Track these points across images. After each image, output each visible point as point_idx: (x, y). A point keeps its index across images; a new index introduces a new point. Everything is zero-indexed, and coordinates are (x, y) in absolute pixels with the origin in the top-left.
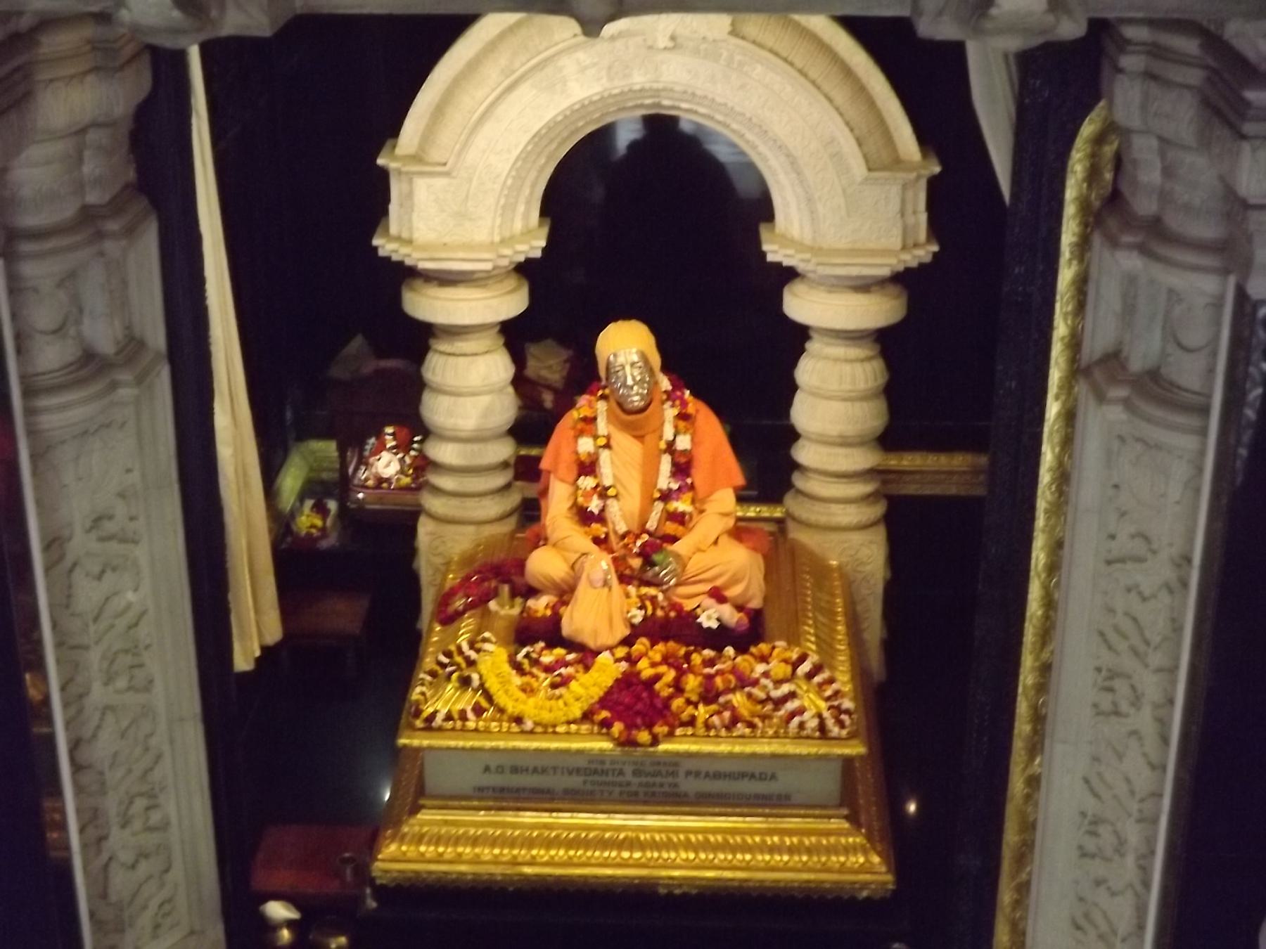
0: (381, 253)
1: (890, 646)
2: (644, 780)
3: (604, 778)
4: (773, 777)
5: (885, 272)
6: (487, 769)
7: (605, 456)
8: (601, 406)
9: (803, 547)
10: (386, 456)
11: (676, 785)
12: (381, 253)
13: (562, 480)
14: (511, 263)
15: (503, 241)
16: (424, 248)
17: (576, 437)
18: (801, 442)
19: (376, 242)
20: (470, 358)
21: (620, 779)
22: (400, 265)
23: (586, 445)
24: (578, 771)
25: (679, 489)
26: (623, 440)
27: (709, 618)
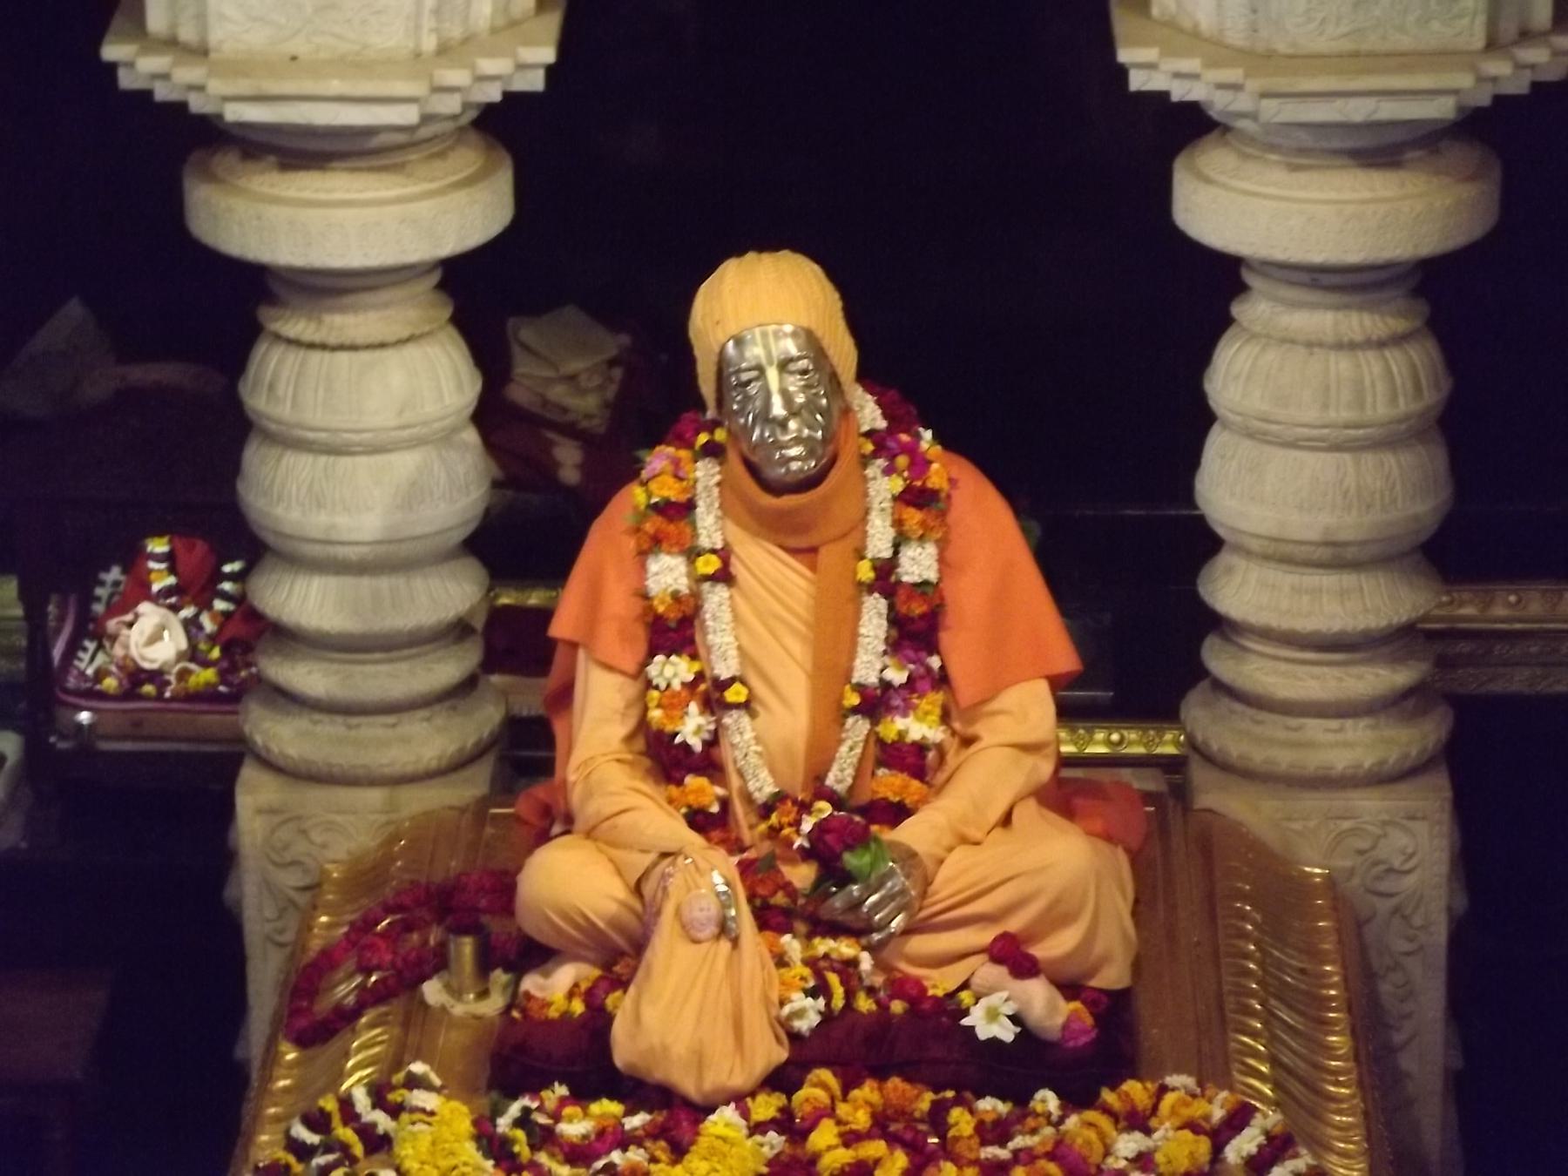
0: (126, 81)
1: (1464, 1087)
5: (1442, 109)
7: (716, 599)
8: (706, 473)
9: (1235, 830)
10: (149, 615)
12: (126, 81)
13: (610, 668)
14: (466, 106)
15: (443, 50)
16: (240, 67)
17: (643, 554)
18: (1224, 559)
19: (111, 51)
20: (364, 356)
22: (178, 109)
23: (667, 574)
25: (910, 684)
26: (760, 560)
27: (992, 1015)
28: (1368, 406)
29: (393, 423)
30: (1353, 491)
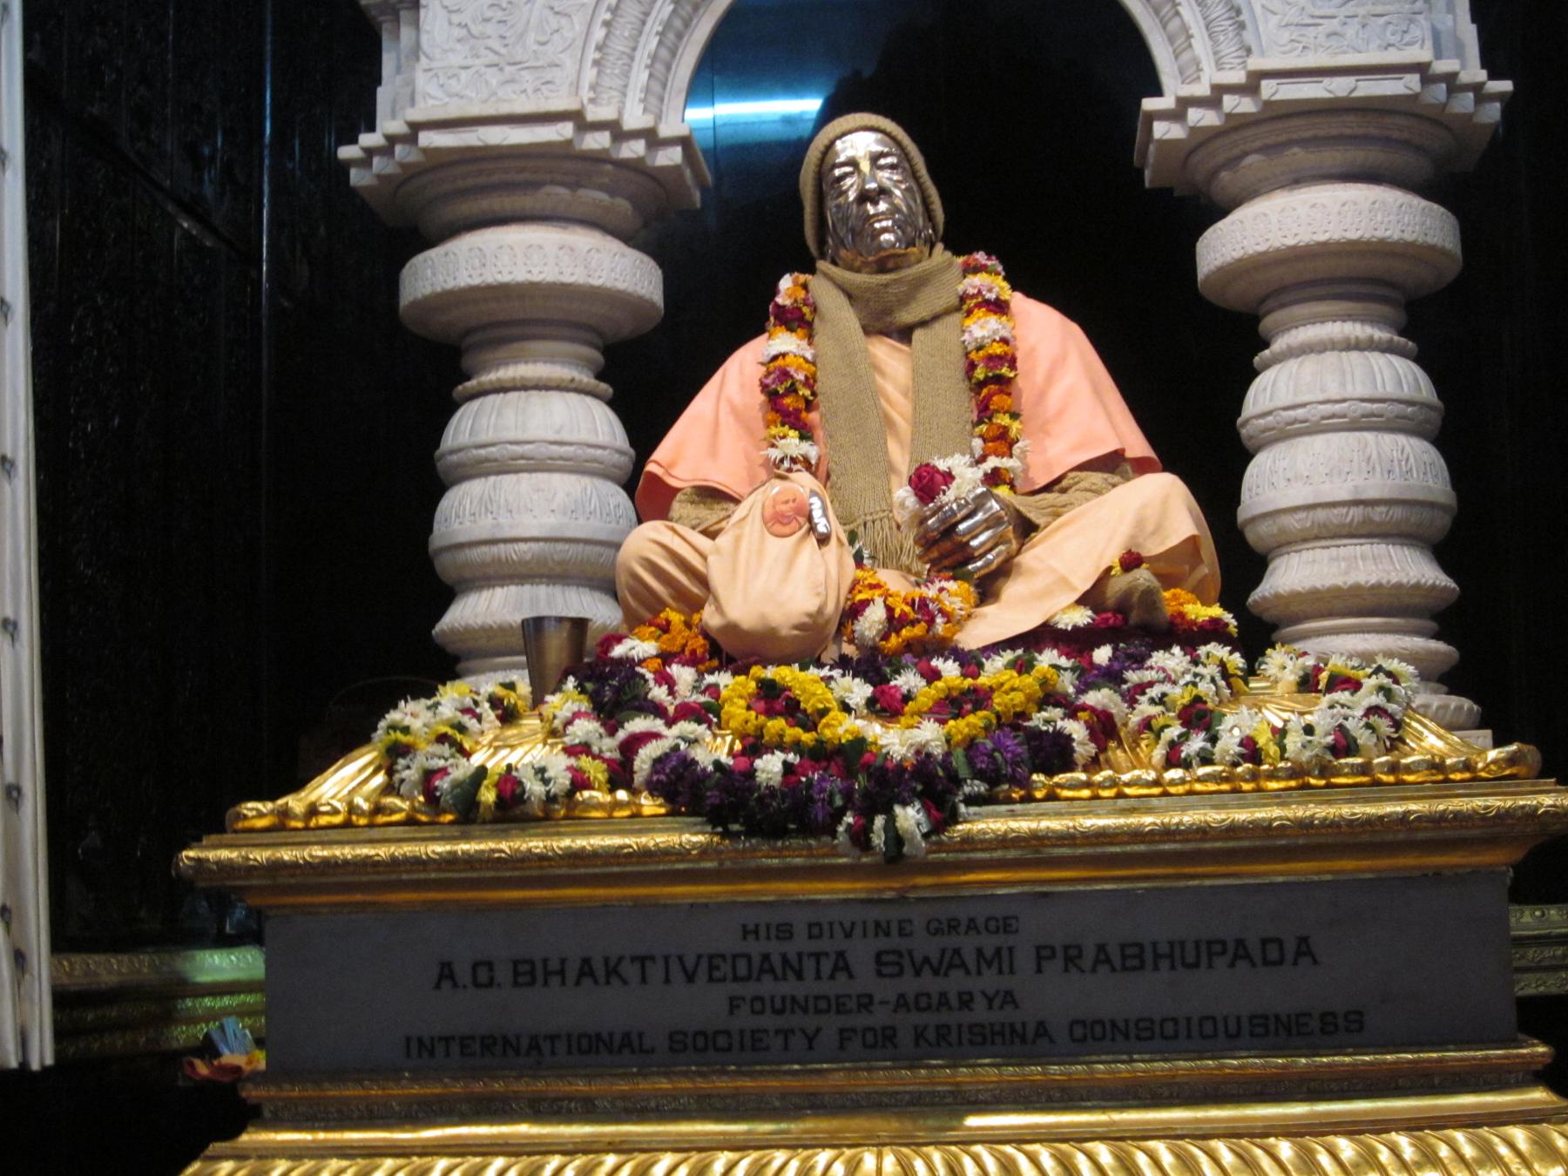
2: (909, 985)
3: (789, 987)
4: (1304, 948)
6: (446, 973)
11: (1009, 998)
21: (840, 985)
24: (714, 965)
28: (1379, 385)
29: (552, 437)
30: (1374, 456)
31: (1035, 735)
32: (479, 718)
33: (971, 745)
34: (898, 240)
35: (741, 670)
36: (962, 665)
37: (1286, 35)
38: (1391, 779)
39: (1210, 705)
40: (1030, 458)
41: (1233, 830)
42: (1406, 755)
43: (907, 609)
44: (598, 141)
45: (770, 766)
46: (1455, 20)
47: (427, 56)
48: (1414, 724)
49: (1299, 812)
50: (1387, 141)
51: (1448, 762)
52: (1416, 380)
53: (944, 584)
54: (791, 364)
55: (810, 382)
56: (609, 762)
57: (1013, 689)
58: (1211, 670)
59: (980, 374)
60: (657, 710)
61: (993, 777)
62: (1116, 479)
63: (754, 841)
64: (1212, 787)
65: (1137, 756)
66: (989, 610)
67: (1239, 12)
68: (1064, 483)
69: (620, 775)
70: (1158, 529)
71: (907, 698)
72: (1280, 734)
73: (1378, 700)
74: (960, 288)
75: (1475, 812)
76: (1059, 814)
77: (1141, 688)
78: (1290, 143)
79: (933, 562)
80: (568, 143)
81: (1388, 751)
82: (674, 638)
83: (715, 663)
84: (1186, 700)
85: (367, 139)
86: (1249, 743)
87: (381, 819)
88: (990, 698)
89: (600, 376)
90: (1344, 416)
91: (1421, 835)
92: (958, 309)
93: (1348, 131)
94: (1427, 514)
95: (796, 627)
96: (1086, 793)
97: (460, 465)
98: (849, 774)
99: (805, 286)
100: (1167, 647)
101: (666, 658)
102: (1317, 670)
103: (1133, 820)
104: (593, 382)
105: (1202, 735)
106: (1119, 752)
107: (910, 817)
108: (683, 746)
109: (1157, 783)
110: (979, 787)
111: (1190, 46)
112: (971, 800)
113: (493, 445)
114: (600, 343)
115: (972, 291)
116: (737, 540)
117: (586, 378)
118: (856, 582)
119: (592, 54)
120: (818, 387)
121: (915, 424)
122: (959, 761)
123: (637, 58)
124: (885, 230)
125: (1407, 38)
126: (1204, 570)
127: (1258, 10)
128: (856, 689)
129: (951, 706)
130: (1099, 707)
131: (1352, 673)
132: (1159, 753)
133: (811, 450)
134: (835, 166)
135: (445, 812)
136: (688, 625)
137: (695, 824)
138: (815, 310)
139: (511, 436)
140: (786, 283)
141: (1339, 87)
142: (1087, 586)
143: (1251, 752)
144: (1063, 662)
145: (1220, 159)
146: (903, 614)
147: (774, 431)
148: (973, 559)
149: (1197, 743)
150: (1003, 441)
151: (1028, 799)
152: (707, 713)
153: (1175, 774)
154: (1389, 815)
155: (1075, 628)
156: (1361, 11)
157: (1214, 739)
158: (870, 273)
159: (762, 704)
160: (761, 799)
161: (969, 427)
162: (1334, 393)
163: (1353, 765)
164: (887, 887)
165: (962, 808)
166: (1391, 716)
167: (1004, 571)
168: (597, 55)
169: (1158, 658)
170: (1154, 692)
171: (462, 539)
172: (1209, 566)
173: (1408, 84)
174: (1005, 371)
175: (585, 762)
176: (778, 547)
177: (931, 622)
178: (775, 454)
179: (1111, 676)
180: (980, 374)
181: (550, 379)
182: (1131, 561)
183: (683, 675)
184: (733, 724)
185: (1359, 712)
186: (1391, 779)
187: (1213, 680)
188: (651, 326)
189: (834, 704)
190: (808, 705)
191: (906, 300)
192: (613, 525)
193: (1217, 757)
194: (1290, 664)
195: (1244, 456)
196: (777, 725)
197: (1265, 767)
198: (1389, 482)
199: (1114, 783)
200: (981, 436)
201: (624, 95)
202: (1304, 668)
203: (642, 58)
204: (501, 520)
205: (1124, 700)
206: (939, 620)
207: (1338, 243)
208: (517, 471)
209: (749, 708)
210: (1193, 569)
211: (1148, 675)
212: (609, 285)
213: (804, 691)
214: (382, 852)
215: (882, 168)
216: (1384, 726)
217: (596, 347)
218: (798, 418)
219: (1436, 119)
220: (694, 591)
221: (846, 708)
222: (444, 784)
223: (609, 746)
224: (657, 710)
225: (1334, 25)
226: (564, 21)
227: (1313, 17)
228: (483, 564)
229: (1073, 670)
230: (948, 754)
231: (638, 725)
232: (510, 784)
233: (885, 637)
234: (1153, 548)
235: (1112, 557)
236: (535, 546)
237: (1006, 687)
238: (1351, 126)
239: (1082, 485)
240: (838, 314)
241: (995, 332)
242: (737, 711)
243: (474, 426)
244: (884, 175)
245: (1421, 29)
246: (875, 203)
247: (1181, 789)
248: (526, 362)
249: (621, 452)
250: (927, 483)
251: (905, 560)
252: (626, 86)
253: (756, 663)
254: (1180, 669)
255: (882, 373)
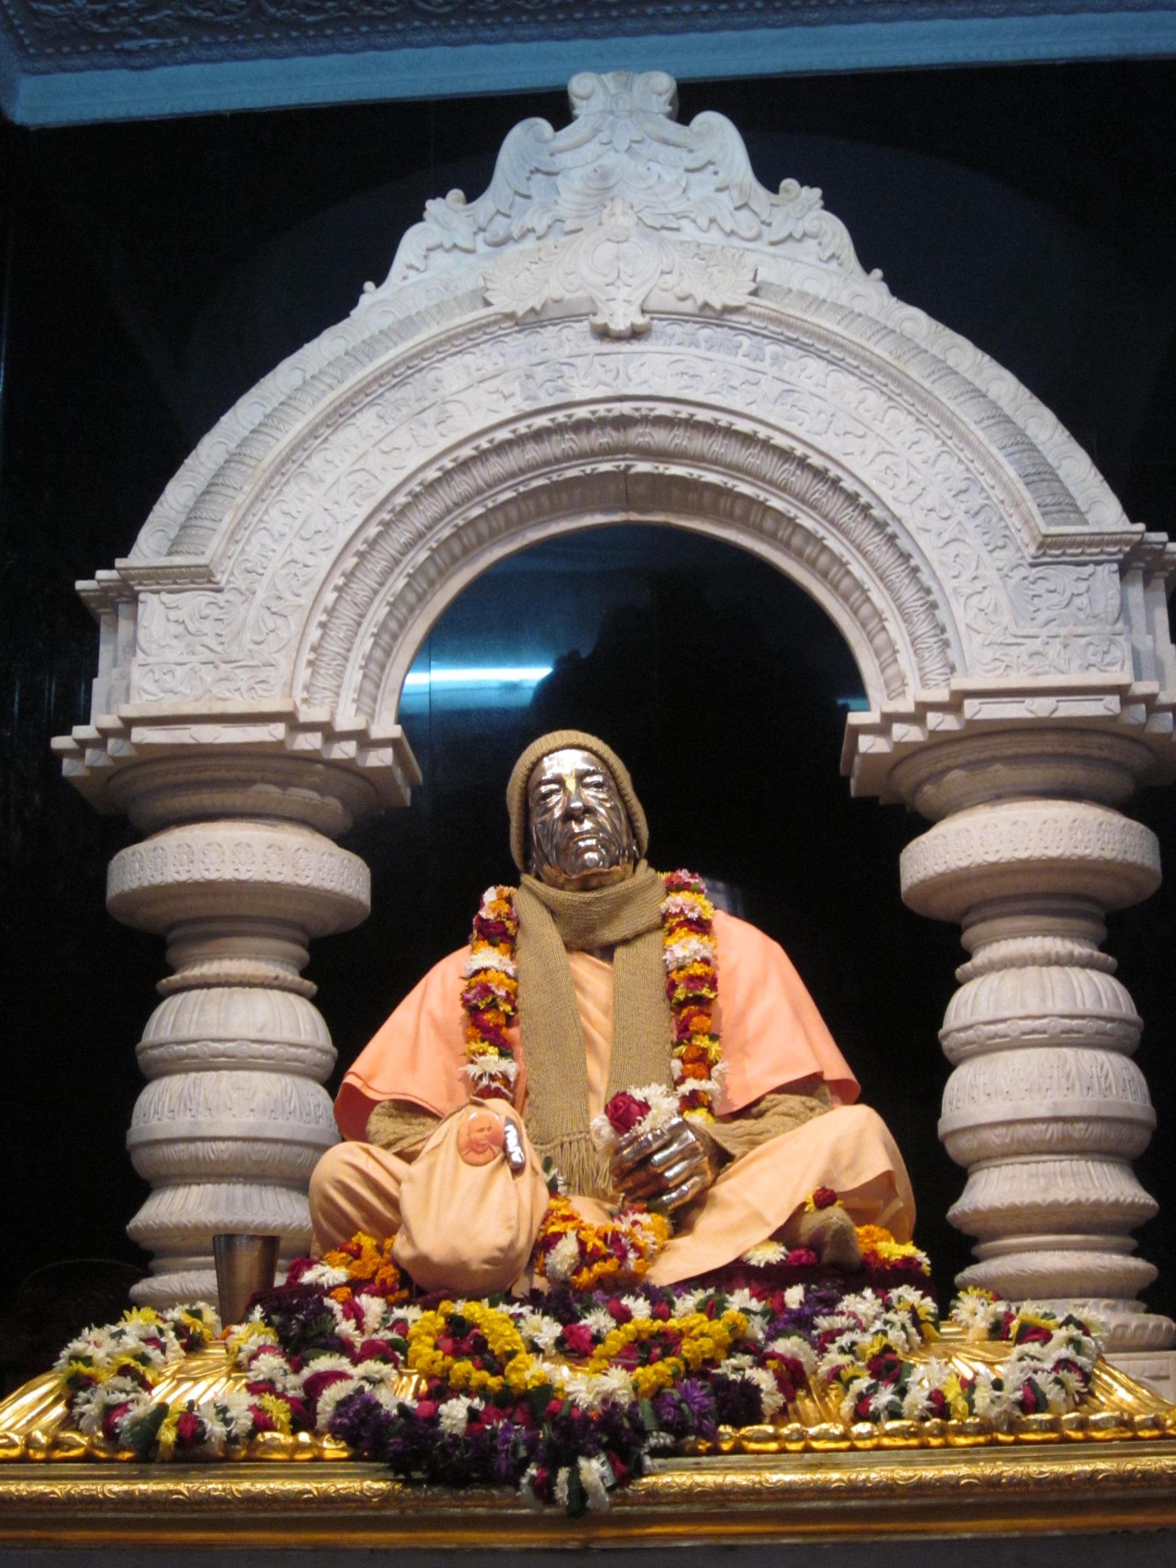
29: (253, 1035)
30: (1074, 1073)
31: (722, 1384)
32: (163, 1348)
33: (658, 1394)
34: (602, 858)
35: (430, 1305)
36: (652, 1304)
37: (989, 654)
38: (1079, 1435)
39: (900, 1355)
40: (729, 1080)
41: (921, 1487)
42: (1097, 1411)
43: (599, 1243)
44: (310, 742)
45: (455, 1411)
46: (1155, 641)
47: (144, 652)
48: (1105, 1377)
49: (987, 1469)
50: (1086, 760)
51: (1137, 1418)
52: (1116, 997)
53: (638, 1217)
54: (492, 979)
55: (511, 998)
56: (292, 1401)
57: (703, 1335)
58: (903, 1317)
59: (680, 994)
60: (343, 1347)
61: (679, 1429)
62: (814, 1102)
63: (436, 1490)
64: (900, 1442)
65: (825, 1405)
66: (682, 1242)
67: (943, 630)
68: (763, 1105)
69: (303, 1416)
70: (853, 1164)
71: (597, 1339)
72: (969, 1386)
73: (1067, 1352)
74: (663, 906)
75: (1163, 1471)
76: (745, 1469)
77: (831, 1335)
78: (994, 760)
79: (628, 1192)
80: (280, 743)
81: (1076, 1407)
82: (365, 1265)
83: (405, 1294)
84: (876, 1349)
85: (81, 732)
86: (937, 1396)
87: (58, 1454)
88: (678, 1343)
89: (304, 974)
90: (1044, 1032)
91: (1109, 1495)
92: (660, 927)
93: (1049, 749)
94: (1125, 1130)
95: (488, 1261)
96: (773, 1446)
97: (164, 1060)
98: (533, 1423)
99: (509, 900)
100: (857, 1290)
101: (356, 1285)
102: (1009, 1317)
103: (820, 1476)
104: (298, 979)
105: (891, 1388)
106: (807, 1401)
107: (594, 1469)
108: (368, 1387)
109: (844, 1437)
110: (665, 1439)
111: (896, 661)
112: (656, 1452)
113: (195, 1041)
114: (306, 940)
115: (674, 910)
116: (431, 1168)
117: (290, 976)
118: (549, 1213)
119: (307, 655)
120: (519, 1003)
121: (617, 1043)
122: (645, 1411)
123: (351, 660)
124: (589, 849)
125: (1108, 659)
126: (899, 1204)
127: (962, 628)
128: (545, 1329)
129: (641, 1350)
130: (788, 1356)
131: (1043, 1323)
132: (847, 1405)
133: (510, 1067)
134: (542, 783)
135: (124, 1449)
136: (380, 1249)
137: (378, 1470)
138: (518, 925)
139: (214, 1032)
140: (490, 896)
141: (1040, 708)
142: (780, 1222)
143: (939, 1406)
144: (755, 1305)
145: (924, 773)
146: (596, 1249)
147: (474, 1046)
148: (667, 1191)
149: (885, 1396)
150: (702, 1063)
151: (715, 1451)
152: (392, 1352)
153: (863, 1428)
154: (1077, 1474)
155: (769, 1265)
156: (1063, 631)
157: (902, 1392)
158: (571, 890)
159: (448, 1343)
160: (443, 1448)
161: (668, 1047)
162: (1034, 1008)
163: (1041, 1422)
164: (572, 1539)
165: (648, 1461)
166: (1080, 1369)
167: (700, 1201)
168: (312, 656)
169: (850, 1302)
170: (844, 1340)
171: (160, 1135)
172: (904, 1199)
173: (1109, 705)
174: (705, 991)
175: (268, 1401)
176: (472, 1176)
177: (623, 1257)
178: (474, 1070)
179: (801, 1322)
180: (680, 994)
181: (255, 977)
182: (825, 1198)
183: (373, 1306)
184: (420, 1363)
185: (1048, 1365)
186: (1079, 1435)
187: (903, 1327)
188: (357, 923)
189: (521, 1347)
190: (496, 1346)
191: (609, 917)
192: (313, 1125)
193: (905, 1411)
194: (981, 1310)
195: (943, 1067)
196: (463, 1367)
197: (954, 1422)
198: (1088, 1099)
199: (801, 1436)
200: (680, 1058)
201: (338, 695)
202: (995, 1315)
203: (357, 658)
204: (201, 1118)
205: (814, 1347)
206: (632, 1255)
207: (1039, 860)
208: (217, 1068)
209: (436, 1347)
210: (887, 1203)
211: (839, 1322)
212: (315, 884)
213: (492, 1331)
214: (58, 1489)
215: (587, 786)
216: (1073, 1381)
217: (302, 944)
218: (498, 1035)
219: (1135, 738)
220: (386, 1220)
221: (534, 1348)
222: (123, 1421)
223: (293, 1383)
224: (343, 1347)
225: (1036, 645)
226: (280, 621)
227: (1016, 636)
228: (180, 1162)
229: (763, 1314)
230: (634, 1405)
231: (324, 1363)
232: (190, 1421)
233: (577, 1271)
234: (848, 1183)
235: (806, 1192)
236: (231, 1145)
237: (695, 1332)
238: (1051, 744)
239: (779, 1109)
240: (540, 930)
241: (696, 953)
242: (424, 1350)
243: (174, 1021)
244: (589, 794)
245: (1121, 651)
246: (580, 822)
247: (868, 1444)
248: (231, 959)
249: (323, 1051)
250: (624, 1112)
251: (601, 1184)
252: (339, 687)
253: (446, 1298)
254: (871, 1313)
255: (582, 990)
